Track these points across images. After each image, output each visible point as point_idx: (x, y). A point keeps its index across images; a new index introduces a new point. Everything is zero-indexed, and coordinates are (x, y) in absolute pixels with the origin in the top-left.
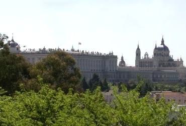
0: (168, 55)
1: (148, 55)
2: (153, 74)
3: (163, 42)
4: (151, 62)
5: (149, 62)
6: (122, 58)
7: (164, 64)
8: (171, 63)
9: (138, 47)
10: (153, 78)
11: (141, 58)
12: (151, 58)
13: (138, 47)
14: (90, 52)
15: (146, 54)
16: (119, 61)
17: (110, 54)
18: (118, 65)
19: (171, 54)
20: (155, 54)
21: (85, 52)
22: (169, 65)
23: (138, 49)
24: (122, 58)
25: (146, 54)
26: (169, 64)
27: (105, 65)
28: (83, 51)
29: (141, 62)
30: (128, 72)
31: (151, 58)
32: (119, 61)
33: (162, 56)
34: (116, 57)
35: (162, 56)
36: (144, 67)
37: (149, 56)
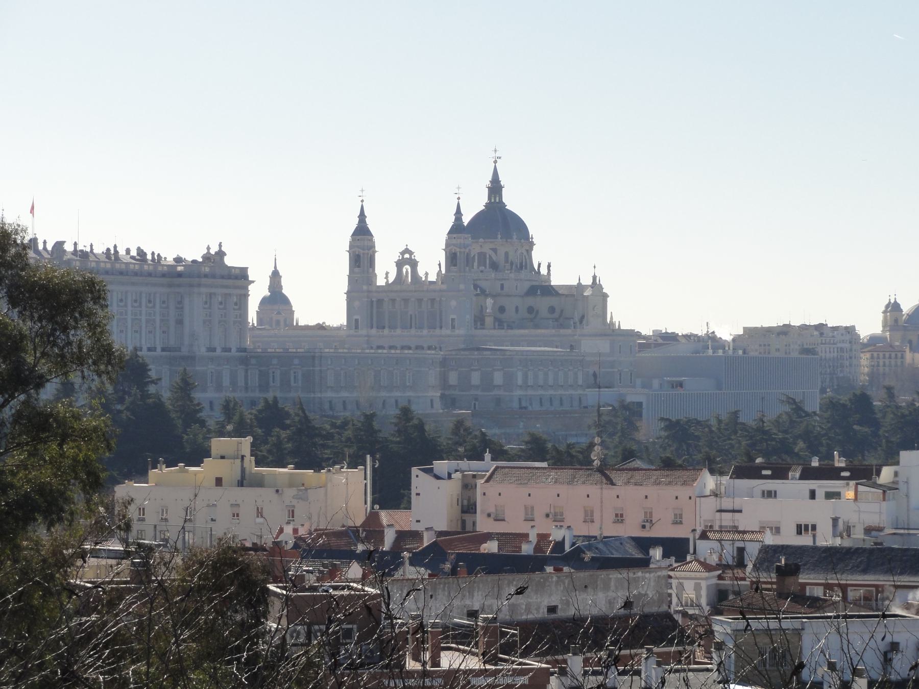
0: (525, 263)
1: (414, 264)
2: (444, 363)
3: (495, 188)
4: (433, 300)
5: (420, 301)
6: (275, 276)
7: (502, 309)
8: (542, 304)
9: (362, 216)
10: (444, 384)
11: (381, 282)
12: (433, 278)
13: (362, 216)
14: (99, 250)
15: (407, 260)
16: (257, 292)
17: (207, 257)
18: (252, 316)
19: (538, 257)
20: (452, 258)
21: (69, 247)
22: (532, 318)
23: (362, 232)
24: (275, 276)
25: (407, 260)
26: (530, 310)
27: (180, 322)
28: (59, 245)
29: (380, 302)
30: (311, 358)
31: (433, 278)
32: (257, 292)
33: (494, 266)
34: (241, 277)
35: (494, 266)
36: (392, 327)
37: (421, 272)
